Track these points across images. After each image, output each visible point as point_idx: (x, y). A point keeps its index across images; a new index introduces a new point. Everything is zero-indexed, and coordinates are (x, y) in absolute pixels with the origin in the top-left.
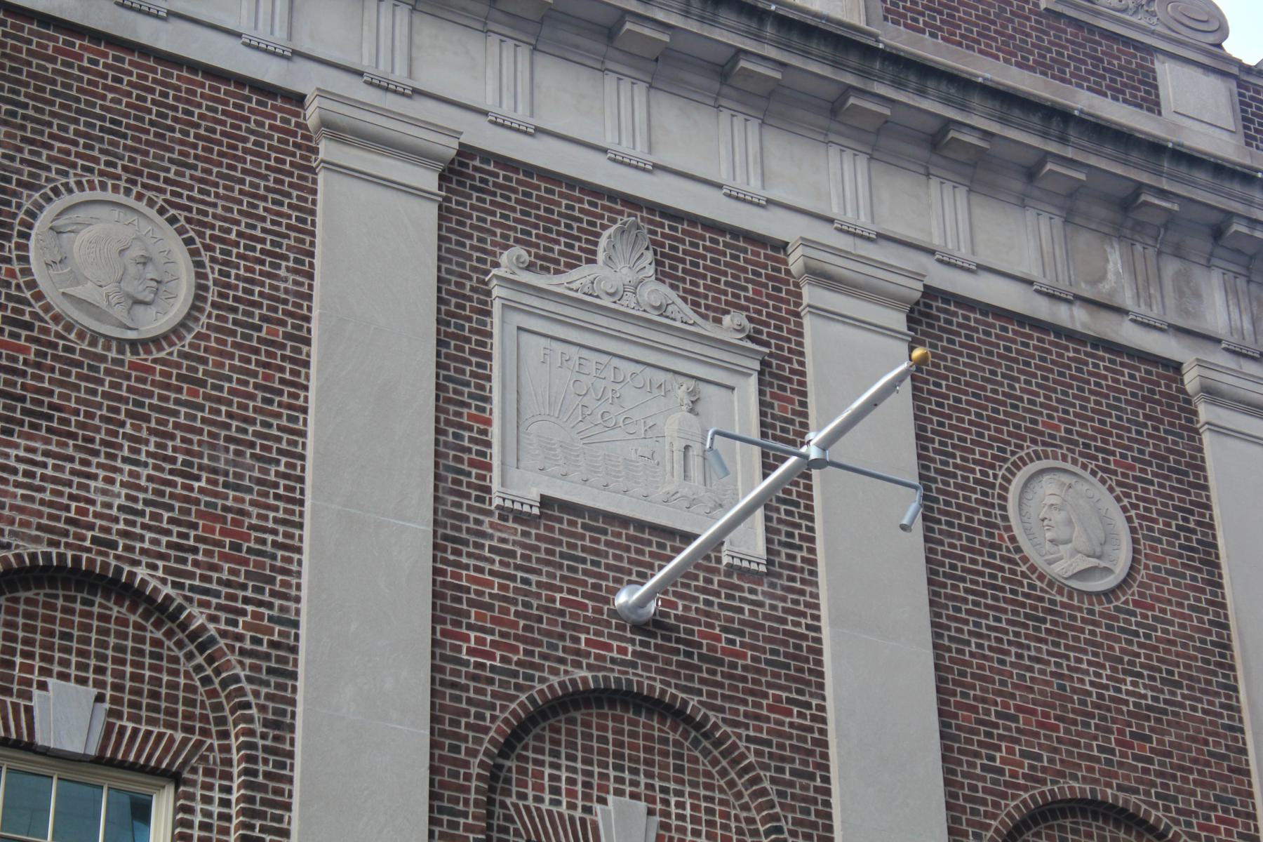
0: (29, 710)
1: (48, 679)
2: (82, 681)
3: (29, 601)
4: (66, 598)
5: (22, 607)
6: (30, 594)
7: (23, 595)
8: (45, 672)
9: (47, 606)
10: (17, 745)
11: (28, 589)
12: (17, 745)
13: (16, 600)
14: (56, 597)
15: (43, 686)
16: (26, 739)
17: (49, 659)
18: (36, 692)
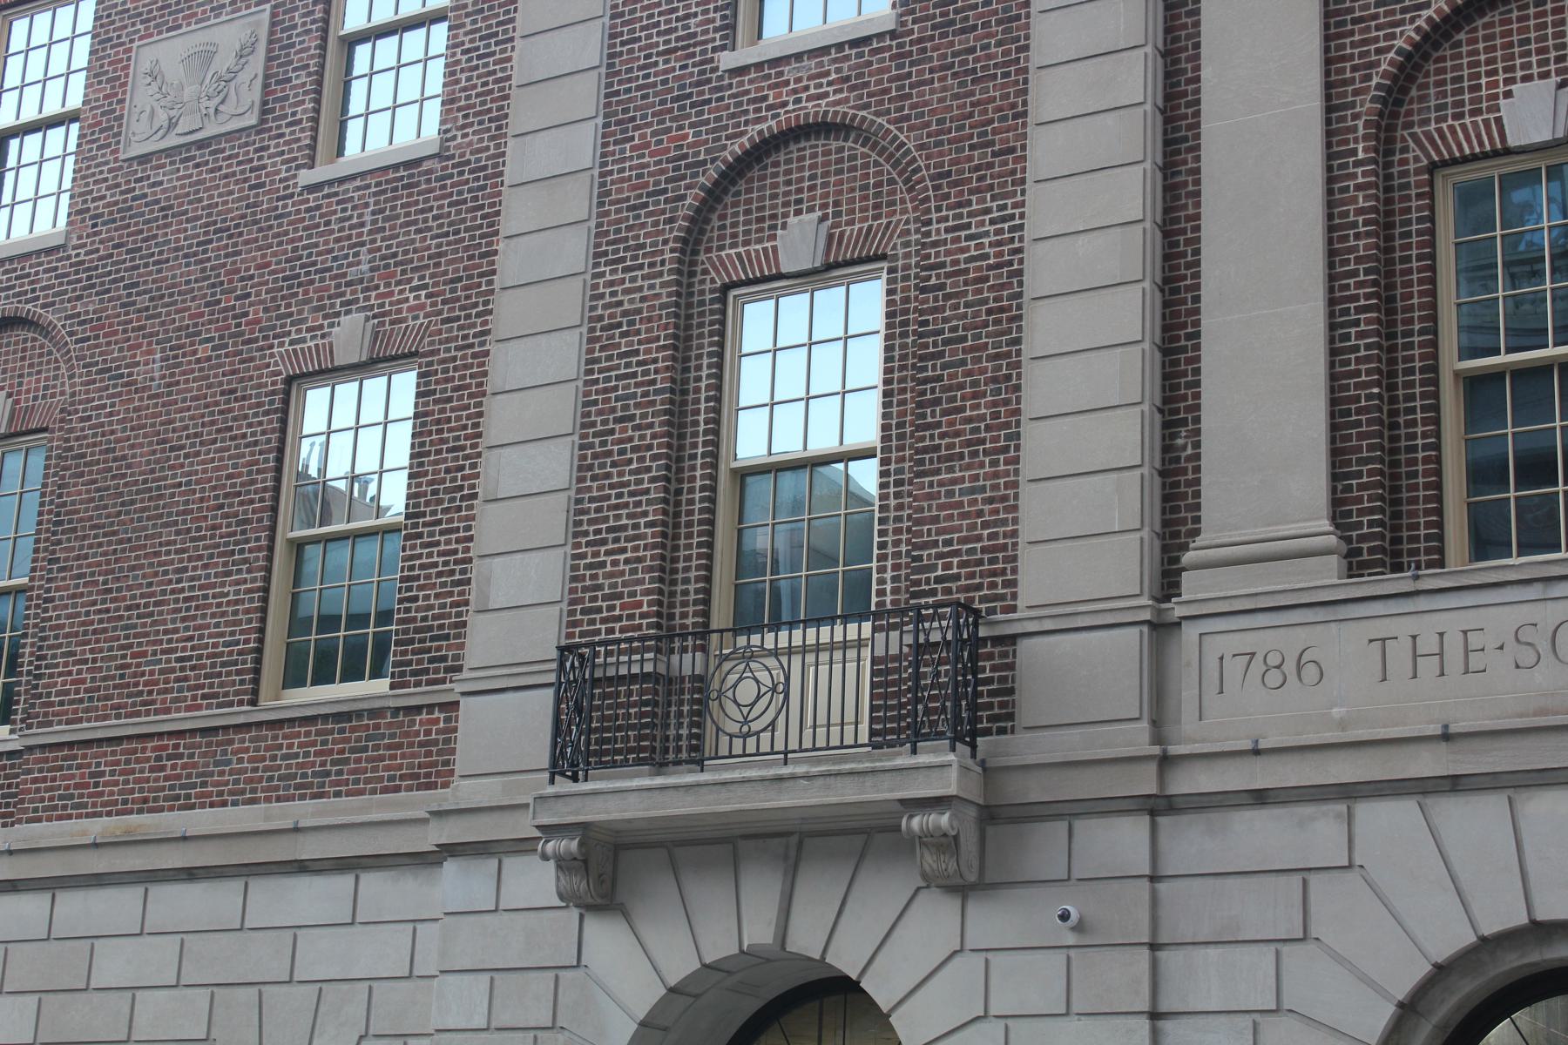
0: (1499, 120)
1: (1513, 87)
2: (1544, 76)
3: (1485, 26)
4: (1520, 8)
5: (1481, 33)
6: (1486, 19)
7: (1480, 22)
8: (1512, 81)
9: (1503, 22)
10: (1495, 154)
11: (1482, 14)
12: (1495, 154)
13: (1475, 30)
14: (1510, 11)
15: (1508, 94)
16: (1499, 146)
17: (1512, 69)
18: (1502, 102)
